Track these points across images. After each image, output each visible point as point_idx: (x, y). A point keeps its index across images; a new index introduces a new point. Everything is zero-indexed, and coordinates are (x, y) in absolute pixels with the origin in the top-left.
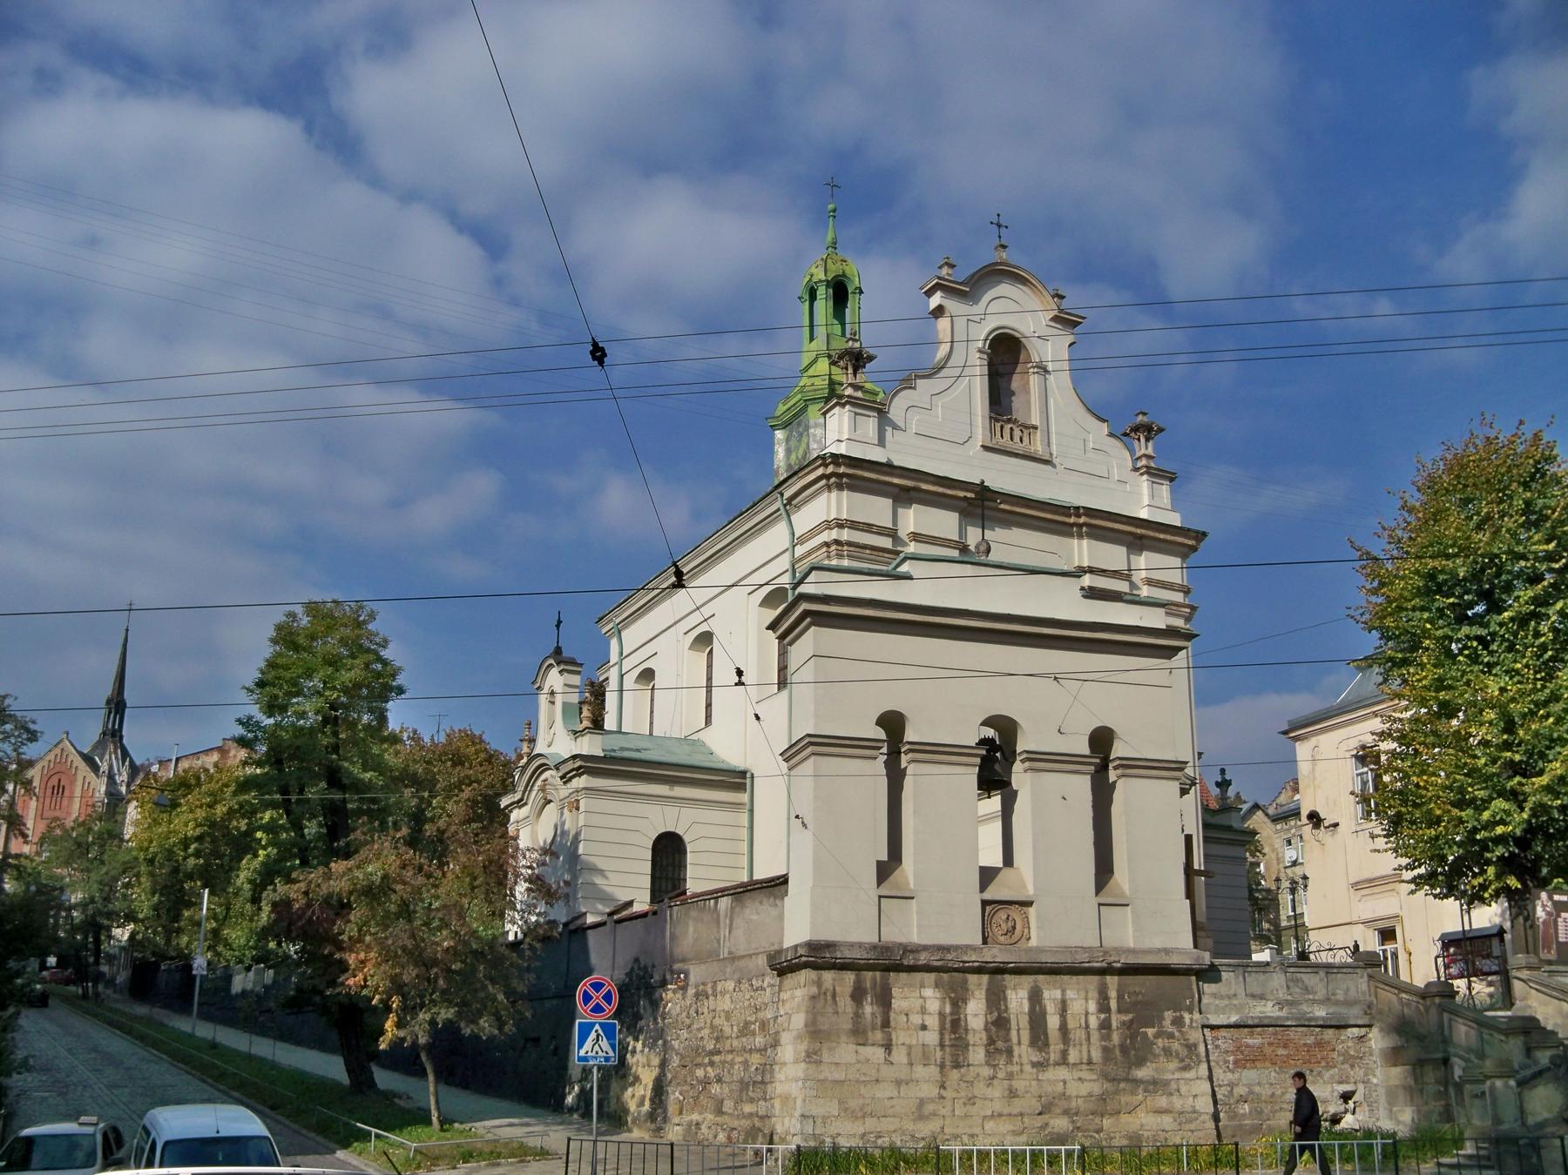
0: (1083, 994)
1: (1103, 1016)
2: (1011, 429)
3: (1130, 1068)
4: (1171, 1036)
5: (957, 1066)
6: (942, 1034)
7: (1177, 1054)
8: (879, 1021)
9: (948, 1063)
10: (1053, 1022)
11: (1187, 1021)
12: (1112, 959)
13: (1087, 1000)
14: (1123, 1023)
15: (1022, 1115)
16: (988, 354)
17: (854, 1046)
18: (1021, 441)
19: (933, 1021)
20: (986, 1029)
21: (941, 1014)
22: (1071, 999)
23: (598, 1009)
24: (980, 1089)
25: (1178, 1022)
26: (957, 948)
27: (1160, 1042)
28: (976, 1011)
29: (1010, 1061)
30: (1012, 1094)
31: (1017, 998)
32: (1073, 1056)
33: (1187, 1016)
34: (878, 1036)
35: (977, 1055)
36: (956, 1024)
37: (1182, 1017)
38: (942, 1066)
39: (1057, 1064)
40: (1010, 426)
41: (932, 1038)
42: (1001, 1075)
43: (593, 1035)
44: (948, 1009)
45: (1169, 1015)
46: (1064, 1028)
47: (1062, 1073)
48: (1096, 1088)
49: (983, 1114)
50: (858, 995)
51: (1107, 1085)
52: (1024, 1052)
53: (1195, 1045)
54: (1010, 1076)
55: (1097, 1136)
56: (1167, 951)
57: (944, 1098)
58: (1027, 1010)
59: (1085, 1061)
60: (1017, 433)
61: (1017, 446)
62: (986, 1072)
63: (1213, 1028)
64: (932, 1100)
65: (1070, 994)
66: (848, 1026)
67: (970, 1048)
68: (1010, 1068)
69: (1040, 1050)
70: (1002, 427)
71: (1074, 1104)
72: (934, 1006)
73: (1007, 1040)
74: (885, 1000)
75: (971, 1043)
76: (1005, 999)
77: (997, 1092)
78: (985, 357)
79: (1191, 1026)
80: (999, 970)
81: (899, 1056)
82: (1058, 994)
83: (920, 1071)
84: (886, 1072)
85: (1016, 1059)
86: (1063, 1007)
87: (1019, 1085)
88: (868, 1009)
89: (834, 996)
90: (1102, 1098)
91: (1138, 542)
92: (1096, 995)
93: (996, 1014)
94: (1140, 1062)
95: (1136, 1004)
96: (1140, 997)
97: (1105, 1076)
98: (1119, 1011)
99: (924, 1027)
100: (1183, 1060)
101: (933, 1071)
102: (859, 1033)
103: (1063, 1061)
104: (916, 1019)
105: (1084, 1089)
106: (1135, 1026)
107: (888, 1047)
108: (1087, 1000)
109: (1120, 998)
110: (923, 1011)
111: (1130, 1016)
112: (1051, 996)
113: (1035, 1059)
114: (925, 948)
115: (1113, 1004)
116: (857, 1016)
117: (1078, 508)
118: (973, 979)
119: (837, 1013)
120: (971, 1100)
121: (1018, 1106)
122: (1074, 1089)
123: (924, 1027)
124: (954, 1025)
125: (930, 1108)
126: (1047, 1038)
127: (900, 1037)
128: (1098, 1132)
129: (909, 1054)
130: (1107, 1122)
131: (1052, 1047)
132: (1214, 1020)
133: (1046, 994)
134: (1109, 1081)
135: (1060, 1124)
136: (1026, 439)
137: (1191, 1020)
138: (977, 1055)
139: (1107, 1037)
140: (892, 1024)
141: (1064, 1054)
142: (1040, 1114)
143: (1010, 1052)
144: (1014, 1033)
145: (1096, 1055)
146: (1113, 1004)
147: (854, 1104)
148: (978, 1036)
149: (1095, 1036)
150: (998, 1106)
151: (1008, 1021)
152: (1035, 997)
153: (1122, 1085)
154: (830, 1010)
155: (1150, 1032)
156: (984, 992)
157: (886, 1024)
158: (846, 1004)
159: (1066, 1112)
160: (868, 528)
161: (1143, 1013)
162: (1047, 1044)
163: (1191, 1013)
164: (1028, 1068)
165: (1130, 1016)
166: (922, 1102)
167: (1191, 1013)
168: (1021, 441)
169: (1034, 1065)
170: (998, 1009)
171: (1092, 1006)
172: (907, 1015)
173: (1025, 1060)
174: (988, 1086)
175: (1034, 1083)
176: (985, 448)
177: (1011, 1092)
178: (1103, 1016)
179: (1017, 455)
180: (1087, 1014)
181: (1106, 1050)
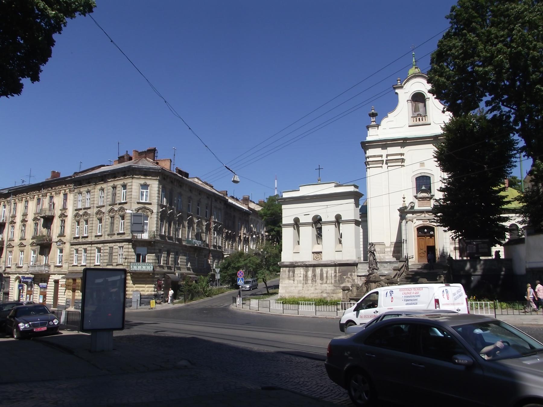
0: (331, 270)
1: (335, 274)
2: (419, 119)
3: (340, 284)
4: (349, 278)
5: (306, 284)
6: (303, 278)
7: (350, 282)
8: (292, 276)
9: (304, 283)
10: (325, 275)
11: (353, 275)
12: (335, 262)
13: (332, 271)
14: (339, 275)
15: (318, 293)
17: (288, 280)
19: (302, 276)
20: (312, 277)
21: (304, 274)
22: (329, 271)
23: (241, 276)
24: (310, 288)
25: (351, 275)
26: (305, 262)
27: (347, 279)
28: (310, 273)
29: (316, 283)
30: (316, 289)
32: (328, 282)
33: (353, 274)
34: (292, 278)
35: (310, 282)
36: (306, 276)
37: (352, 274)
38: (303, 284)
39: (325, 283)
40: (418, 117)
41: (302, 279)
42: (314, 285)
43: (240, 280)
44: (305, 273)
45: (349, 274)
46: (327, 276)
47: (326, 285)
48: (333, 288)
49: (310, 293)
50: (289, 271)
51: (335, 288)
52: (319, 281)
53: (354, 280)
54: (315, 286)
55: (332, 298)
56: (348, 260)
57: (303, 290)
58: (320, 273)
59: (331, 283)
61: (421, 122)
62: (311, 285)
63: (360, 276)
64: (301, 290)
65: (328, 270)
66: (287, 276)
67: (309, 281)
68: (316, 284)
69: (322, 281)
71: (328, 291)
72: (302, 273)
73: (316, 279)
74: (294, 272)
75: (309, 279)
76: (316, 271)
77: (313, 289)
79: (354, 275)
80: (314, 266)
81: (296, 282)
82: (326, 270)
83: (299, 285)
84: (294, 285)
85: (317, 282)
87: (317, 287)
88: (291, 273)
89: (285, 271)
90: (334, 290)
92: (334, 270)
93: (314, 274)
94: (342, 283)
95: (342, 271)
96: (343, 270)
97: (334, 286)
98: (339, 273)
99: (300, 277)
100: (351, 283)
101: (301, 285)
102: (289, 278)
103: (326, 283)
104: (299, 275)
105: (330, 288)
106: (342, 276)
107: (294, 280)
108: (332, 271)
109: (339, 270)
110: (300, 274)
111: (341, 274)
113: (321, 282)
114: (299, 262)
115: (337, 271)
116: (289, 275)
118: (309, 268)
119: (285, 274)
120: (308, 290)
121: (317, 291)
122: (328, 288)
123: (300, 277)
124: (306, 276)
125: (300, 292)
126: (323, 278)
127: (296, 279)
128: (332, 297)
129: (297, 282)
130: (334, 295)
131: (324, 280)
132: (359, 274)
133: (324, 270)
134: (335, 287)
135: (325, 295)
136: (424, 119)
137: (354, 274)
138: (310, 282)
139: (336, 278)
140: (295, 276)
141: (327, 281)
142: (321, 293)
143: (316, 281)
144: (317, 278)
145: (333, 282)
146: (337, 271)
147: (288, 291)
148: (310, 278)
149: (333, 278)
150: (313, 291)
151: (316, 275)
152: (322, 271)
153: (338, 288)
154: (284, 274)
155: (345, 277)
156: (312, 270)
157: (294, 276)
158: (287, 272)
159: (327, 293)
161: (344, 273)
162: (323, 280)
163: (354, 273)
164: (319, 284)
165: (341, 274)
166: (299, 290)
167: (354, 273)
169: (321, 284)
170: (314, 273)
171: (333, 272)
172: (297, 274)
173: (319, 283)
174: (312, 287)
175: (320, 287)
176: (410, 126)
177: (315, 288)
178: (335, 274)
180: (332, 273)
181: (335, 281)
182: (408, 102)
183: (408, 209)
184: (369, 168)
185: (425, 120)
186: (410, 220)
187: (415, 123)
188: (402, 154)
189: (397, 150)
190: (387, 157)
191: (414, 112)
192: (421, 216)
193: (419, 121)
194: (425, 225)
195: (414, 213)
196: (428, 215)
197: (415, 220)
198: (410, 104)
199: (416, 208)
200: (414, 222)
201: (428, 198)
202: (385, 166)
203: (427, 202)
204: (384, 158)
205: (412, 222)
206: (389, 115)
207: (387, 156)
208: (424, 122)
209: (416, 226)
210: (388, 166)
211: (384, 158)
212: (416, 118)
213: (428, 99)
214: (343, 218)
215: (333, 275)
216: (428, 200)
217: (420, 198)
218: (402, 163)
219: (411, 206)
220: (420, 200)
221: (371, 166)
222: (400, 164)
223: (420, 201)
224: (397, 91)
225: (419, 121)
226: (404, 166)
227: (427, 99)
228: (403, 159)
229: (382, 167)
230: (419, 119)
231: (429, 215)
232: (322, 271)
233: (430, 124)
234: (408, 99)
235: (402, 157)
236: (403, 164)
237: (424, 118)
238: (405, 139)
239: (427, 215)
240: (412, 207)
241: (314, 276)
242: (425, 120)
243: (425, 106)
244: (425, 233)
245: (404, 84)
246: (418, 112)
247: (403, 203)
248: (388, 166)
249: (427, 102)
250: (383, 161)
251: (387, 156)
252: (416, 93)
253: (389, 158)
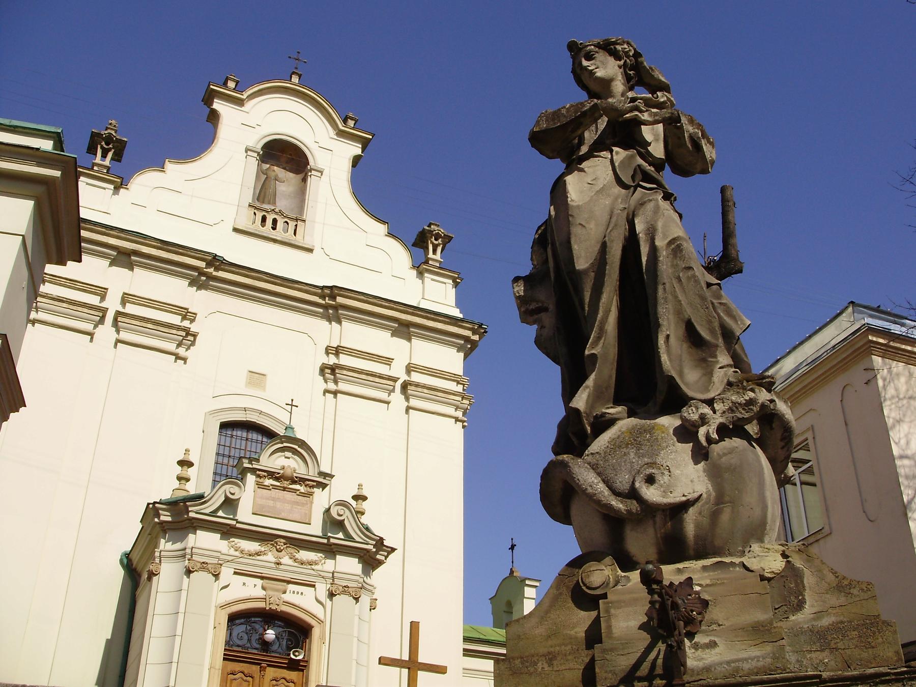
2: (275, 221)
16: (258, 154)
60: (280, 225)
61: (278, 234)
70: (264, 219)
78: (256, 155)
91: (405, 329)
117: (331, 288)
176: (236, 230)
179: (275, 241)
182: (249, 153)
183: (207, 511)
184: (34, 322)
185: (295, 234)
186: (204, 566)
187: (257, 228)
188: (186, 314)
190: (124, 302)
191: (258, 200)
192: (258, 558)
193: (274, 228)
194: (274, 607)
195: (228, 532)
196: (291, 562)
197: (226, 573)
198: (253, 163)
199: (245, 515)
200: (223, 581)
201: (302, 481)
202: (106, 332)
203: (297, 503)
204: (113, 304)
205: (217, 576)
206: (169, 166)
207: (126, 299)
208: (289, 236)
209: (229, 604)
210: (118, 341)
211: (113, 304)
212: (264, 219)
213: (319, 174)
216: (303, 495)
217: (271, 475)
218: (177, 348)
219: (227, 498)
220: (268, 482)
221: (41, 316)
222: (172, 347)
223: (266, 488)
224: (218, 105)
225: (274, 228)
226: (185, 360)
227: (313, 173)
228: (188, 332)
229: (91, 335)
230: (275, 221)
231: (295, 560)
233: (310, 250)
234: (251, 144)
235: (186, 323)
236: (181, 351)
237: (292, 224)
238: (215, 261)
239: (286, 560)
240: (230, 504)
242: (295, 234)
243: (302, 192)
244: (265, 645)
245: (252, 96)
246: (269, 203)
247: (176, 484)
248: (118, 341)
249: (312, 181)
250: (104, 311)
251: (126, 299)
252: (275, 140)
253: (131, 309)
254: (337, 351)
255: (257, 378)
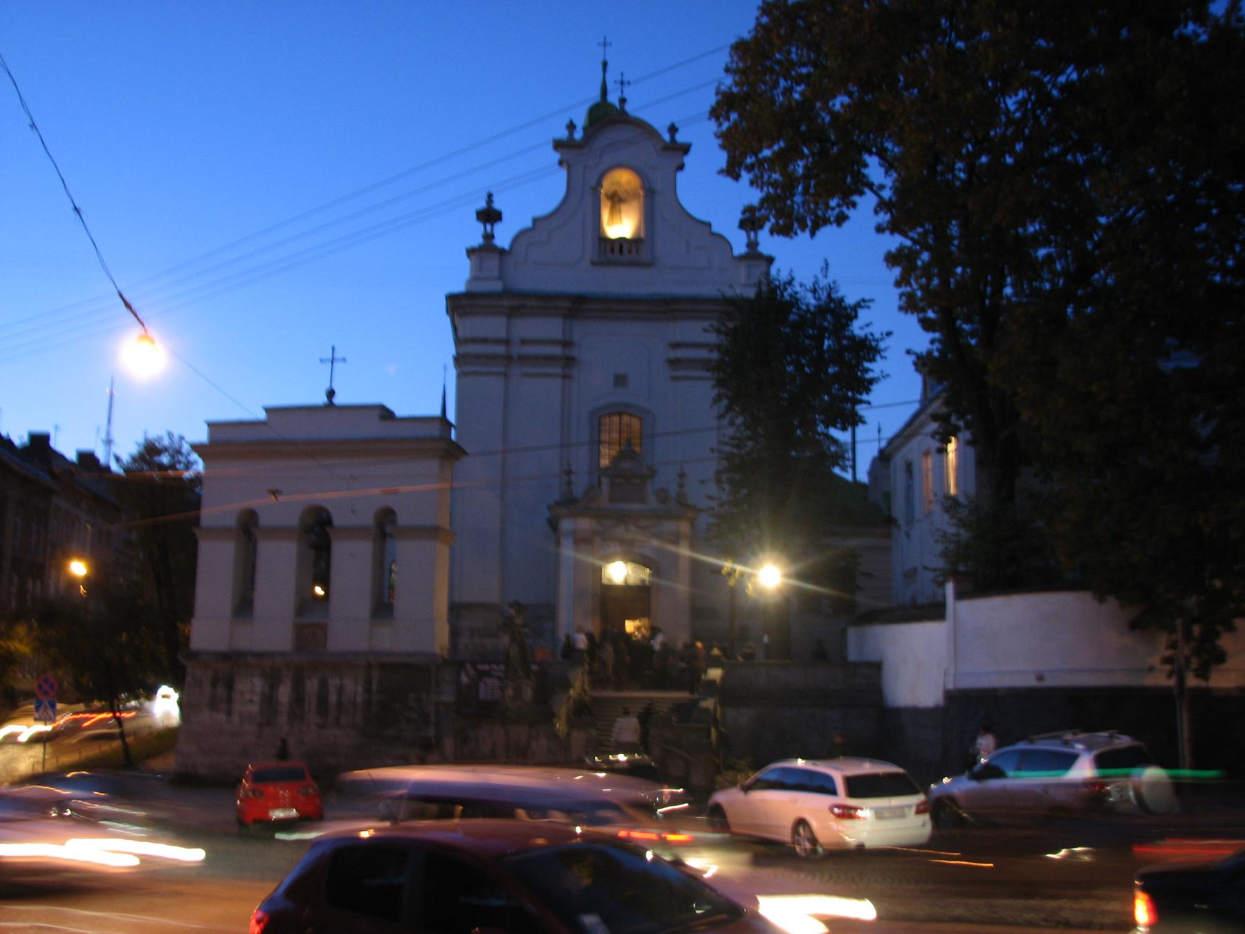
10: (333, 698)
18: (630, 251)
19: (256, 698)
28: (284, 693)
31: (312, 685)
35: (283, 718)
41: (255, 709)
50: (214, 683)
74: (230, 686)
81: (236, 719)
86: (341, 690)
88: (221, 691)
99: (251, 701)
102: (213, 705)
107: (229, 713)
112: (334, 682)
115: (374, 687)
123: (251, 701)
124: (269, 700)
136: (634, 250)
138: (283, 718)
152: (323, 684)
157: (230, 701)
158: (208, 689)
160: (485, 341)
168: (630, 251)
171: (360, 689)
189: (550, 327)
214: (403, 519)
215: (359, 699)
232: (323, 684)
241: (298, 698)
254: (676, 346)
255: (620, 380)
